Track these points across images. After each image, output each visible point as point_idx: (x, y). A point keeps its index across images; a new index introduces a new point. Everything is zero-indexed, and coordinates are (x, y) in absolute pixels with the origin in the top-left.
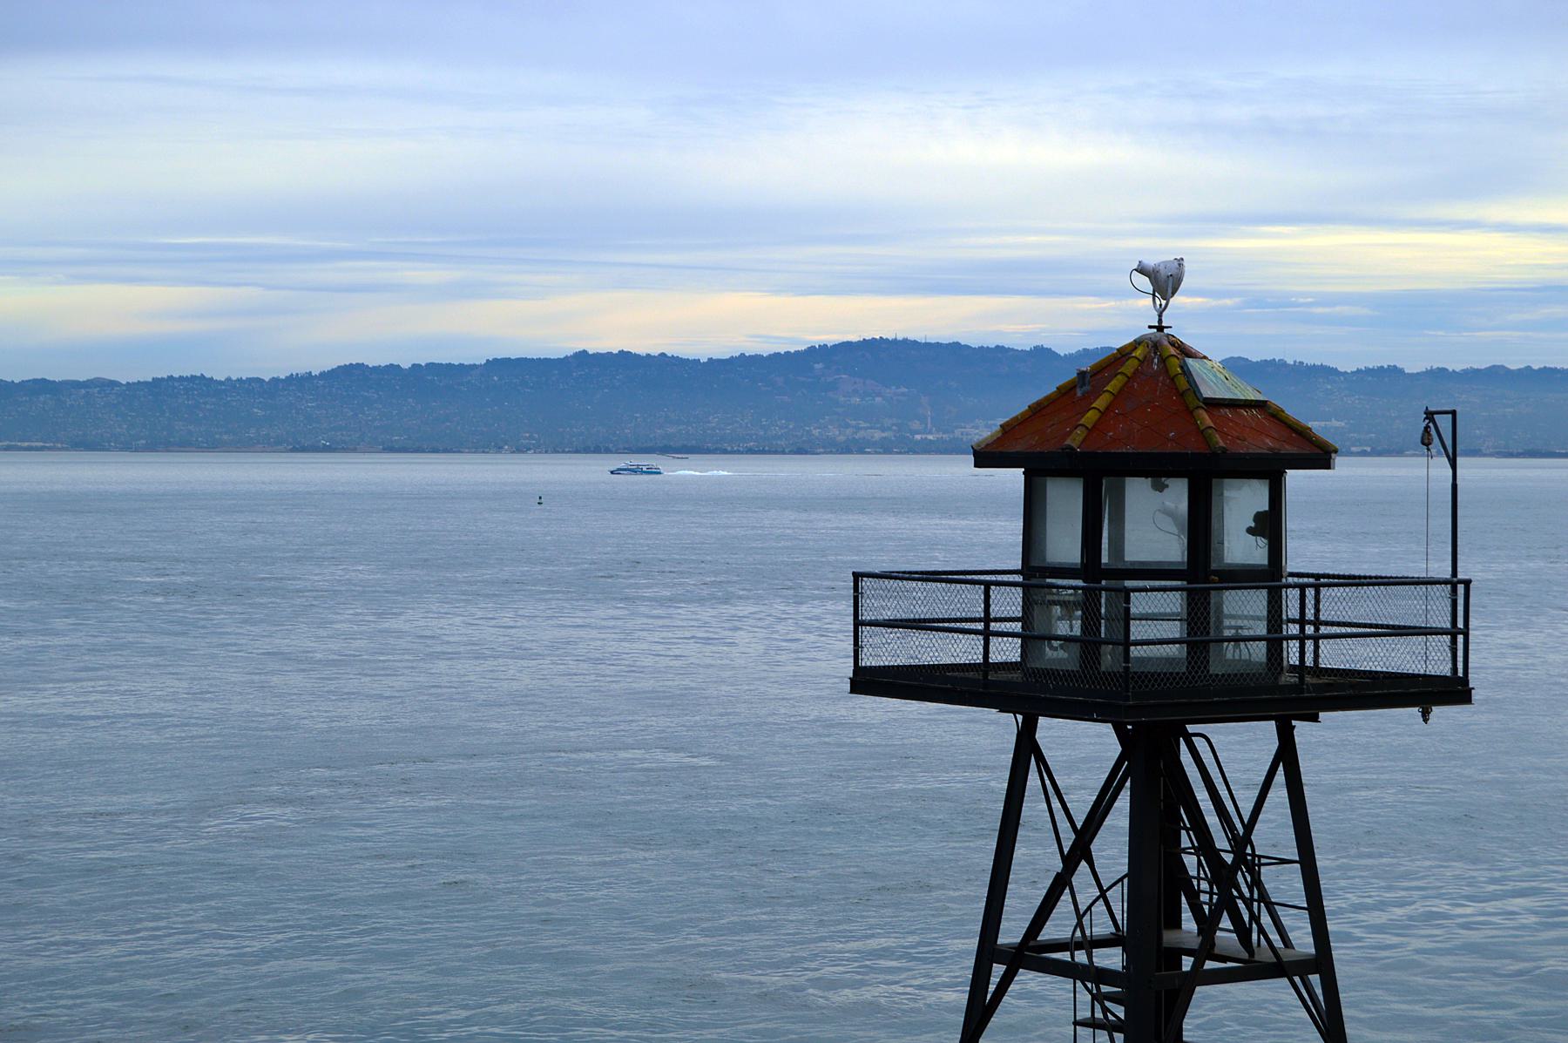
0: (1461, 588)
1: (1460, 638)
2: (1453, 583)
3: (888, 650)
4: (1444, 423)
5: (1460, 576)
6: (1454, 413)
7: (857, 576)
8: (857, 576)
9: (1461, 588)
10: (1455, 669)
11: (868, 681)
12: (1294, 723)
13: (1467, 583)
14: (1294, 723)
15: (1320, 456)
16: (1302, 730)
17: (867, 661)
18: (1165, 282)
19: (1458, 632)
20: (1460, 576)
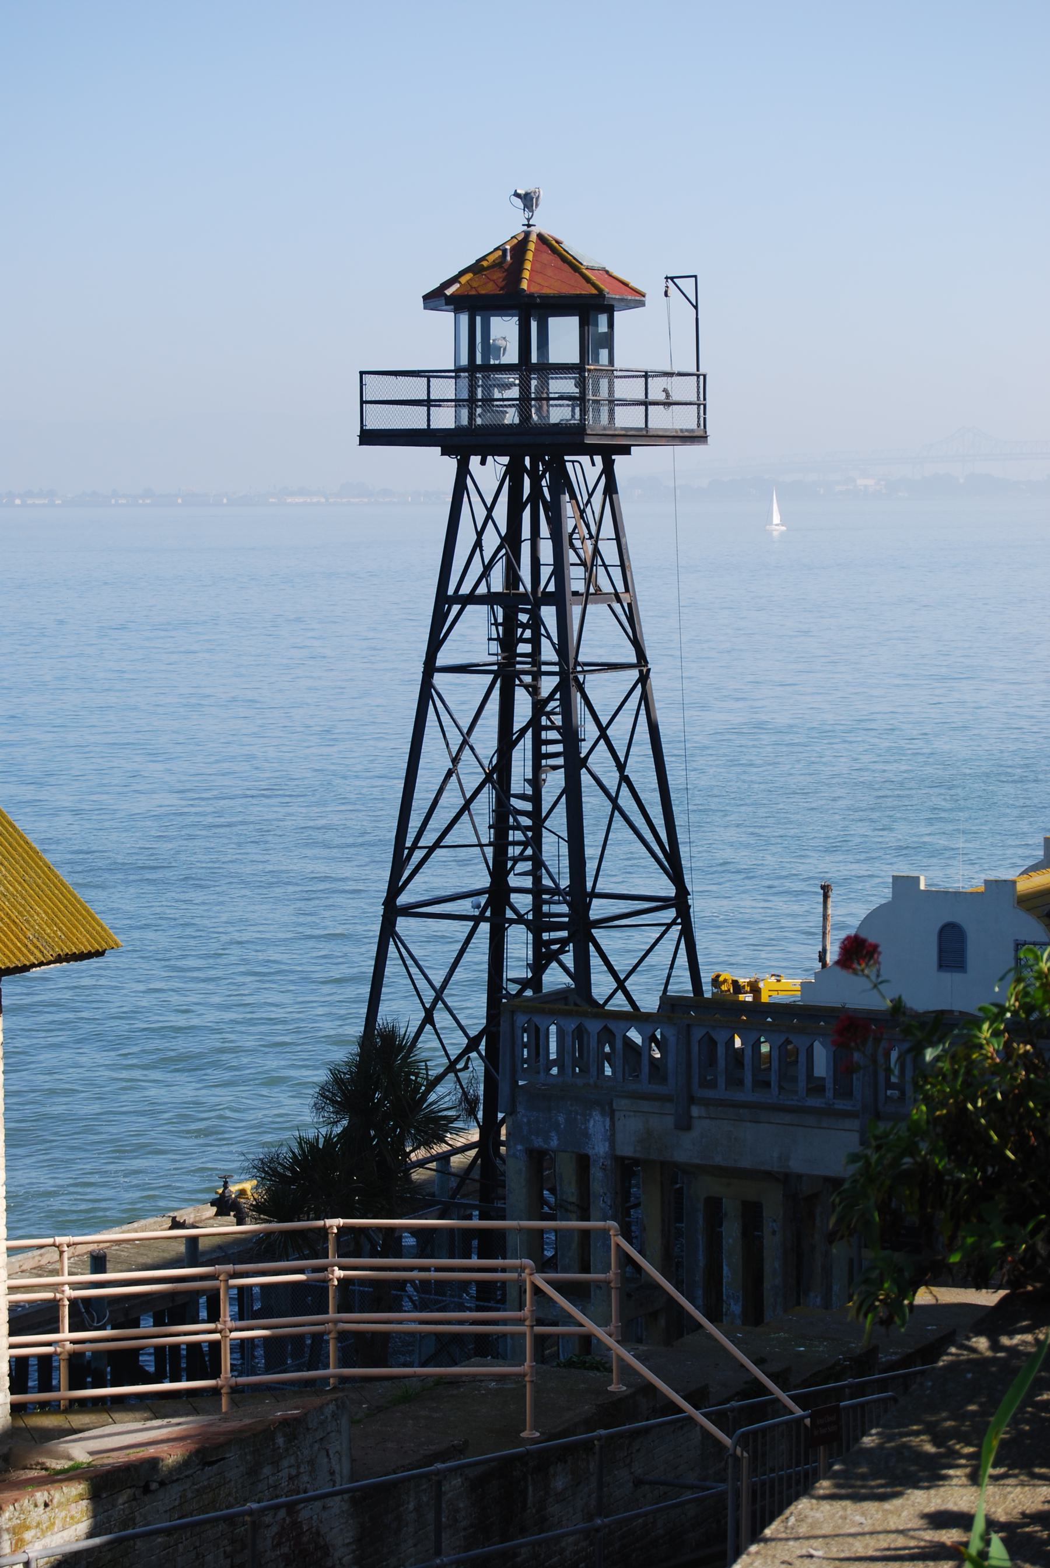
0: (702, 378)
1: (702, 407)
2: (698, 376)
3: (381, 419)
4: (687, 285)
5: (702, 371)
6: (695, 277)
7: (362, 373)
8: (362, 373)
9: (702, 378)
10: (699, 425)
11: (369, 437)
12: (613, 457)
13: (705, 376)
14: (613, 457)
15: (636, 299)
16: (619, 460)
17: (370, 425)
18: (528, 200)
19: (701, 404)
20: (702, 371)
